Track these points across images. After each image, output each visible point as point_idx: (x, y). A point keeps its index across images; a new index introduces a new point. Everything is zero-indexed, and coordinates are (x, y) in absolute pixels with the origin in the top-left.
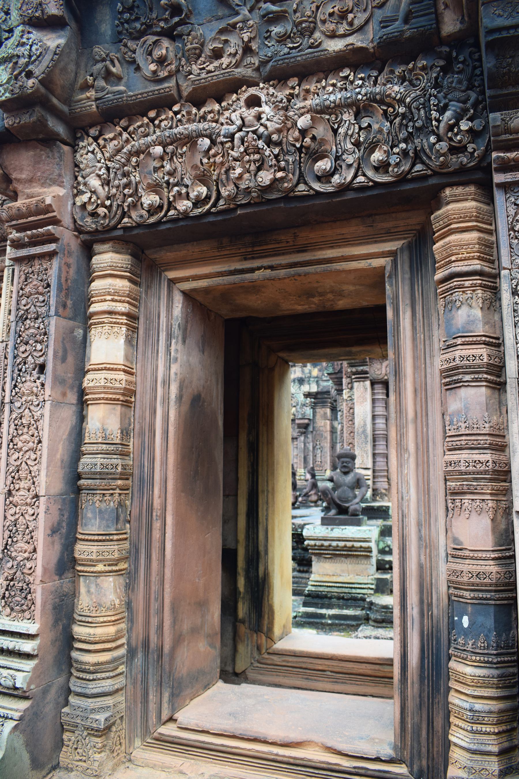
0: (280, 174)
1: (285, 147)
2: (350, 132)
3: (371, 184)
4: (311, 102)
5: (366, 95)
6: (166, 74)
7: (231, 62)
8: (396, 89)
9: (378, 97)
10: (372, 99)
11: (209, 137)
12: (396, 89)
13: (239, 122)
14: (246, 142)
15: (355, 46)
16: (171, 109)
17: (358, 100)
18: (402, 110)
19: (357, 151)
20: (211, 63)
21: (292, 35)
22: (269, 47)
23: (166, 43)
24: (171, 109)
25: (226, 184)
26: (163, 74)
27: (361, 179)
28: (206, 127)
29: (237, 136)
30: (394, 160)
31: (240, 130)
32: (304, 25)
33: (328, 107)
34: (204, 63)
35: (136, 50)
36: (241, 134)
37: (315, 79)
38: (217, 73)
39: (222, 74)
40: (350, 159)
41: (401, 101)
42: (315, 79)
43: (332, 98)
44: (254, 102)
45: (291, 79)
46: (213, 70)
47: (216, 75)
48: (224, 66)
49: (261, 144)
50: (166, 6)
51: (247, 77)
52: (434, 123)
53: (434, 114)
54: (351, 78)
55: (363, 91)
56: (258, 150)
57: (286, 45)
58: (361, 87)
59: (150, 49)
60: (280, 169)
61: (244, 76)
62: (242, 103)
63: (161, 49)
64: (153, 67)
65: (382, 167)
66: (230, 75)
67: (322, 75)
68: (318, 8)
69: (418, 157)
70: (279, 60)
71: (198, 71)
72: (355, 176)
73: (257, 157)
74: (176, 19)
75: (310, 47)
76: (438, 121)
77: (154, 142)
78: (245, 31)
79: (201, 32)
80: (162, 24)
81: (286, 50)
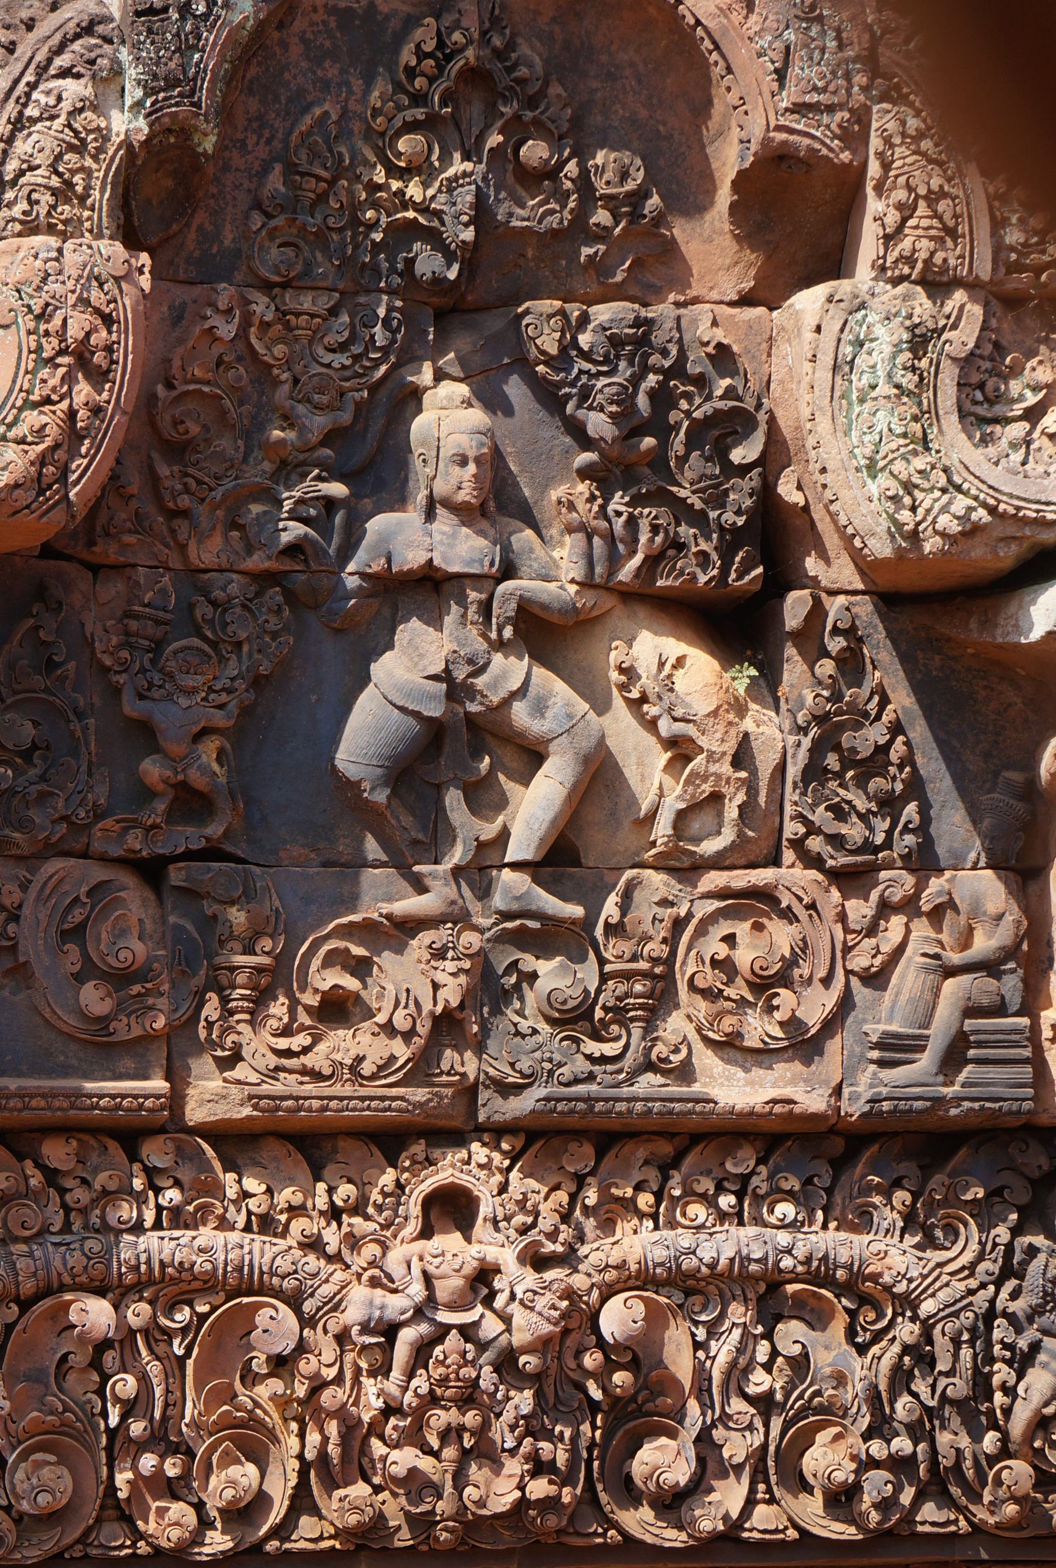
0: (539, 1488)
1: (550, 1391)
2: (742, 1362)
3: (792, 1534)
4: (637, 1243)
5: (808, 1260)
6: (137, 1032)
7: (392, 1058)
8: (891, 1254)
9: (840, 1274)
10: (820, 1272)
11: (294, 1301)
12: (891, 1254)
13: (417, 1290)
14: (442, 1363)
15: (797, 1109)
16: (133, 1156)
17: (780, 1271)
18: (907, 1331)
19: (758, 1423)
20: (317, 1039)
21: (599, 1014)
22: (523, 1036)
23: (134, 901)
24: (133, 1156)
25: (339, 1478)
26: (126, 1029)
27: (763, 1517)
28: (283, 1264)
29: (407, 1336)
30: (877, 1484)
31: (418, 1313)
32: (638, 988)
33: (693, 1274)
34: (286, 1032)
35: (20, 906)
36: (424, 1328)
37: (641, 1153)
38: (338, 1090)
39: (362, 1099)
40: (736, 1447)
41: (908, 1303)
42: (641, 1153)
43: (707, 1253)
44: (452, 1209)
45: (573, 1146)
46: (327, 1071)
47: (341, 1099)
48: (367, 1068)
49: (488, 1378)
50: (161, 787)
51: (437, 1117)
52: (999, 1398)
53: (1002, 1373)
54: (759, 1183)
55: (800, 1252)
56: (469, 1396)
57: (577, 1041)
58: (793, 1226)
59: (77, 916)
60: (539, 1467)
61: (428, 1116)
62: (413, 1207)
63: (123, 933)
64: (94, 998)
65: (841, 1499)
66: (389, 1109)
67: (666, 1149)
68: (679, 925)
69: (937, 1484)
70: (558, 1100)
71: (273, 1061)
72: (751, 1502)
73: (471, 1418)
74: (189, 836)
75: (649, 1066)
76: (1010, 1391)
77: (74, 1277)
78: (450, 966)
79: (277, 903)
80: (134, 841)
81: (581, 1066)
